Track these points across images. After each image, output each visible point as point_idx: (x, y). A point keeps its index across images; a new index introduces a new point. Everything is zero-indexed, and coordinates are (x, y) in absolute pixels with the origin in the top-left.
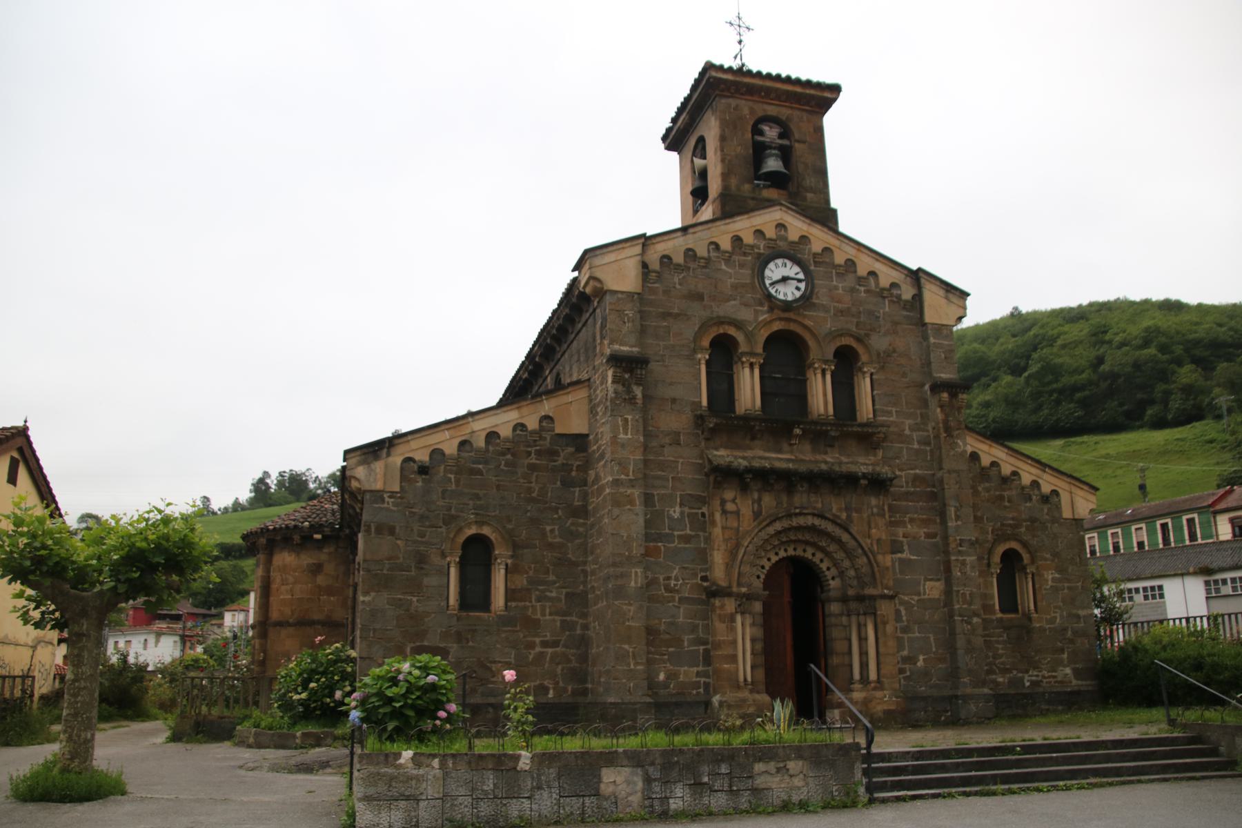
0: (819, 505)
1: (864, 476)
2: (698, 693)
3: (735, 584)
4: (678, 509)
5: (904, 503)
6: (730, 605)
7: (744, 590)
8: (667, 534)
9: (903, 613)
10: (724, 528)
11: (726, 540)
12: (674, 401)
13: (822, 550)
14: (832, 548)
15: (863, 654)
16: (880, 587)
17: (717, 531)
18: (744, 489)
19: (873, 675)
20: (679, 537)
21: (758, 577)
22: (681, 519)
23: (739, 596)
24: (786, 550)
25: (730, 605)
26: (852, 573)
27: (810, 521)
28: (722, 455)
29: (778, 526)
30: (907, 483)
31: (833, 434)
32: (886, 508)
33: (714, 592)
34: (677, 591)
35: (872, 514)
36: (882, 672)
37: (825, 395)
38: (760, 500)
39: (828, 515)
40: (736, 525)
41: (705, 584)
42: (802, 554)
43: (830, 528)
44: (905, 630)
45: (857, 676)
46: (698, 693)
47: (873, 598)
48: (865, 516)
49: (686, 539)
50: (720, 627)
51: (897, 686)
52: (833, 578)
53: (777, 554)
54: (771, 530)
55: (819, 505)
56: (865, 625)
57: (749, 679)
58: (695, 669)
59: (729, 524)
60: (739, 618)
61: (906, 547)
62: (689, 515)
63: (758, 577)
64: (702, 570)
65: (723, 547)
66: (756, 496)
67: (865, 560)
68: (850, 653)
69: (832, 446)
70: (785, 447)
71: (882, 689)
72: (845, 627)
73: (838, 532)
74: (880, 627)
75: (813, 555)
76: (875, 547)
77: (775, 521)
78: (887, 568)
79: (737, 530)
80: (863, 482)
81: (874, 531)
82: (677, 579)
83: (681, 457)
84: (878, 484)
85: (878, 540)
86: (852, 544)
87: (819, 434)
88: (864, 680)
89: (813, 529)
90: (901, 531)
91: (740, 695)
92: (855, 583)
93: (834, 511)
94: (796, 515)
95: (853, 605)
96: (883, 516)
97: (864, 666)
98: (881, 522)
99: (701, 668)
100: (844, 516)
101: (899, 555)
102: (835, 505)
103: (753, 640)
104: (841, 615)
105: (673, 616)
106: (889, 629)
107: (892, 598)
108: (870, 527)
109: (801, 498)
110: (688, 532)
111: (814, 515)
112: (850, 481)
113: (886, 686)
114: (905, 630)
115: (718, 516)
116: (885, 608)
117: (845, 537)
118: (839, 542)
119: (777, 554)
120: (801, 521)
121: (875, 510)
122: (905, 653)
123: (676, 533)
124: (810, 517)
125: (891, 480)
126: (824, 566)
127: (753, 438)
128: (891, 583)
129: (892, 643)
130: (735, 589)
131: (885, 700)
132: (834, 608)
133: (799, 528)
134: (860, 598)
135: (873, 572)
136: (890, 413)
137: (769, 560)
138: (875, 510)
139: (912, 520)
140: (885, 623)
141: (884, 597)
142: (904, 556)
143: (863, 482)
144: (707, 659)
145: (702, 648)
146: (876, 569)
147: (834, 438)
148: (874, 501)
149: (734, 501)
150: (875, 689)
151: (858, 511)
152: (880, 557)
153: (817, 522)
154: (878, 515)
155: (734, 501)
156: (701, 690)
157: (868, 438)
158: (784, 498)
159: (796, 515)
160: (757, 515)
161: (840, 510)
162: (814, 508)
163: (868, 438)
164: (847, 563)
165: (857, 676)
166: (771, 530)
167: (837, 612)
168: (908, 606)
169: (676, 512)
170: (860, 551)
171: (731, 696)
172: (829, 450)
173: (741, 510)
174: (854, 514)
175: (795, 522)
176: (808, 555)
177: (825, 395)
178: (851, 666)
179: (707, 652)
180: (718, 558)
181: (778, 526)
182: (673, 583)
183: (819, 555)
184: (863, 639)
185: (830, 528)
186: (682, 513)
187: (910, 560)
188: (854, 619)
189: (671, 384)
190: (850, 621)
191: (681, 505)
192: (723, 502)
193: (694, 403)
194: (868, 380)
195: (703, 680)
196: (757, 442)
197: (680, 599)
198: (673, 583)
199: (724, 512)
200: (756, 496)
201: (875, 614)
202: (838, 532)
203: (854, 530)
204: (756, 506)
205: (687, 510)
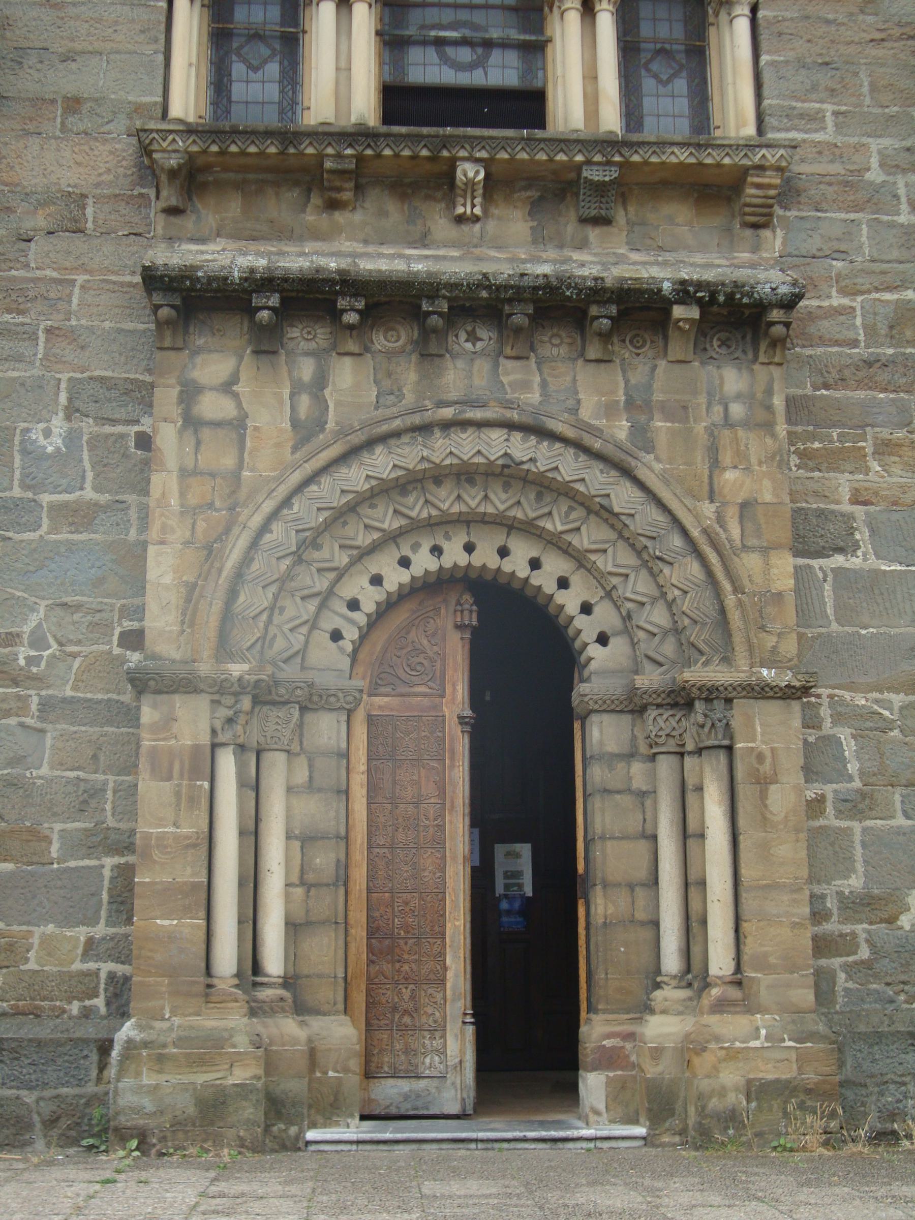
0: (534, 397)
1: (685, 292)
2: (87, 1013)
3: (207, 653)
4: (58, 424)
5: (861, 394)
6: (192, 721)
7: (237, 669)
8: (17, 503)
9: (849, 747)
10: (185, 474)
11: (189, 512)
12: (73, 104)
13: (556, 543)
14: (590, 536)
15: (692, 885)
16: (742, 660)
17: (164, 483)
18: (267, 343)
19: (720, 962)
20: (57, 509)
21: (336, 636)
22: (66, 458)
23: (221, 689)
24: (437, 550)
25: (192, 721)
26: (658, 617)
27: (496, 445)
28: (220, 252)
29: (382, 463)
30: (871, 330)
31: (594, 174)
32: (778, 402)
33: (142, 683)
34: (37, 678)
35: (728, 422)
36: (749, 949)
37: (591, 76)
38: (321, 381)
39: (559, 427)
40: (229, 462)
41: (135, 657)
42: (493, 561)
43: (568, 466)
44: (856, 806)
45: (671, 962)
46: (87, 1013)
47: (711, 694)
48: (700, 428)
49: (79, 516)
50: (153, 792)
51: (806, 996)
52: (603, 640)
53: (405, 563)
54: (355, 477)
55: (534, 397)
56: (700, 789)
57: (274, 962)
58: (82, 933)
59: (206, 459)
60: (227, 764)
61: (862, 535)
62: (95, 442)
63: (336, 636)
64: (125, 613)
65: (180, 533)
66: (307, 369)
67: (695, 568)
68: (655, 881)
69: (603, 221)
70: (440, 225)
71: (749, 1006)
72: (642, 795)
73: (596, 480)
74: (745, 791)
75: (535, 564)
76: (735, 531)
77: (370, 444)
78: (779, 596)
79: (236, 476)
80: (678, 311)
81: (730, 475)
82: (38, 642)
83: (83, 268)
84: (740, 321)
85: (745, 507)
86: (647, 519)
87: (567, 188)
88: (694, 974)
89: (508, 474)
90: (843, 484)
91: (209, 1022)
92: (669, 648)
93: (586, 414)
94: (447, 426)
95: (659, 722)
96: (768, 426)
97: (693, 926)
98: (756, 445)
99: (101, 930)
100: (621, 429)
101: (839, 560)
102: (587, 390)
103: (303, 839)
104: (631, 756)
105: (17, 760)
106: (782, 799)
107: (789, 694)
108: (715, 464)
109: (471, 370)
110: (89, 494)
111: (511, 426)
112: (638, 314)
113: (764, 996)
114: (856, 806)
115: (168, 437)
116: (767, 732)
117: (623, 497)
118: (603, 512)
119: (405, 563)
120: (465, 446)
121: (737, 410)
122: (855, 883)
123: (46, 498)
124: (496, 435)
125: (790, 303)
126: (569, 602)
127: (333, 205)
128: (790, 647)
129: (789, 852)
130: (205, 668)
131: (756, 1045)
132: (602, 734)
133: (466, 474)
134: (681, 700)
135: (723, 611)
136: (815, 119)
137: (377, 580)
138: (737, 410)
139: (885, 448)
140: (763, 782)
141: (762, 692)
142: (855, 562)
143: (678, 311)
144: (123, 901)
145: (109, 862)
146: (730, 600)
147: (600, 189)
148: (733, 379)
149: (228, 387)
150: (720, 1006)
151: (679, 412)
152: (750, 563)
153: (521, 448)
154: (746, 424)
155: (228, 387)
156: (99, 1002)
157: (721, 191)
158: (409, 375)
159: (447, 426)
160: (305, 431)
161: (610, 410)
162: (508, 405)
163: (721, 191)
164: (639, 586)
165: (671, 962)
166: (355, 477)
167: (612, 747)
168: (869, 726)
169: (51, 435)
170: (677, 541)
171: (175, 1022)
172: (593, 234)
173: (256, 410)
174: (659, 424)
175: (442, 449)
176: (517, 565)
177: (591, 76)
178: (655, 924)
179: (125, 874)
180: (163, 569)
181: (382, 463)
182: (23, 653)
183: (555, 565)
184: (690, 836)
185: (568, 466)
186: (71, 438)
187: (877, 574)
188: (665, 767)
189: (68, 58)
190: (653, 776)
191: (71, 412)
192: (190, 392)
193: (138, 109)
194: (742, 26)
195: (106, 967)
196: (340, 217)
197: (46, 706)
198: (23, 653)
199: (192, 423)
200: (307, 369)
201: (730, 749)
202: (596, 480)
203: (650, 468)
204: (305, 401)
205: (88, 427)
